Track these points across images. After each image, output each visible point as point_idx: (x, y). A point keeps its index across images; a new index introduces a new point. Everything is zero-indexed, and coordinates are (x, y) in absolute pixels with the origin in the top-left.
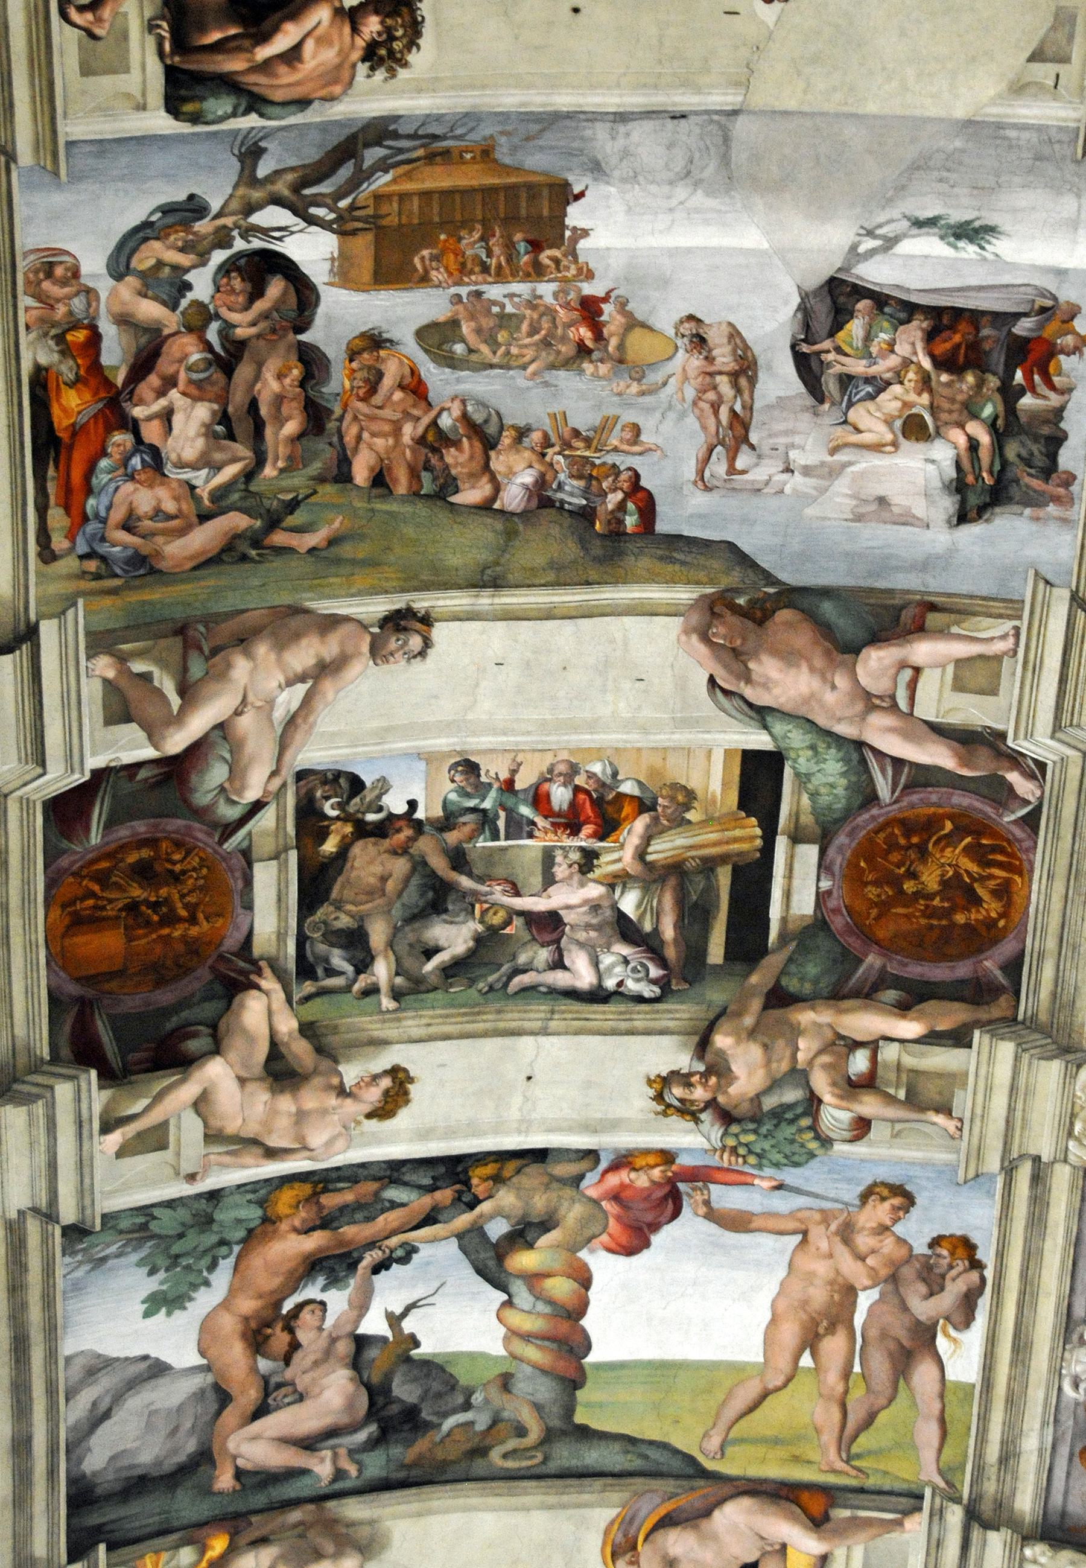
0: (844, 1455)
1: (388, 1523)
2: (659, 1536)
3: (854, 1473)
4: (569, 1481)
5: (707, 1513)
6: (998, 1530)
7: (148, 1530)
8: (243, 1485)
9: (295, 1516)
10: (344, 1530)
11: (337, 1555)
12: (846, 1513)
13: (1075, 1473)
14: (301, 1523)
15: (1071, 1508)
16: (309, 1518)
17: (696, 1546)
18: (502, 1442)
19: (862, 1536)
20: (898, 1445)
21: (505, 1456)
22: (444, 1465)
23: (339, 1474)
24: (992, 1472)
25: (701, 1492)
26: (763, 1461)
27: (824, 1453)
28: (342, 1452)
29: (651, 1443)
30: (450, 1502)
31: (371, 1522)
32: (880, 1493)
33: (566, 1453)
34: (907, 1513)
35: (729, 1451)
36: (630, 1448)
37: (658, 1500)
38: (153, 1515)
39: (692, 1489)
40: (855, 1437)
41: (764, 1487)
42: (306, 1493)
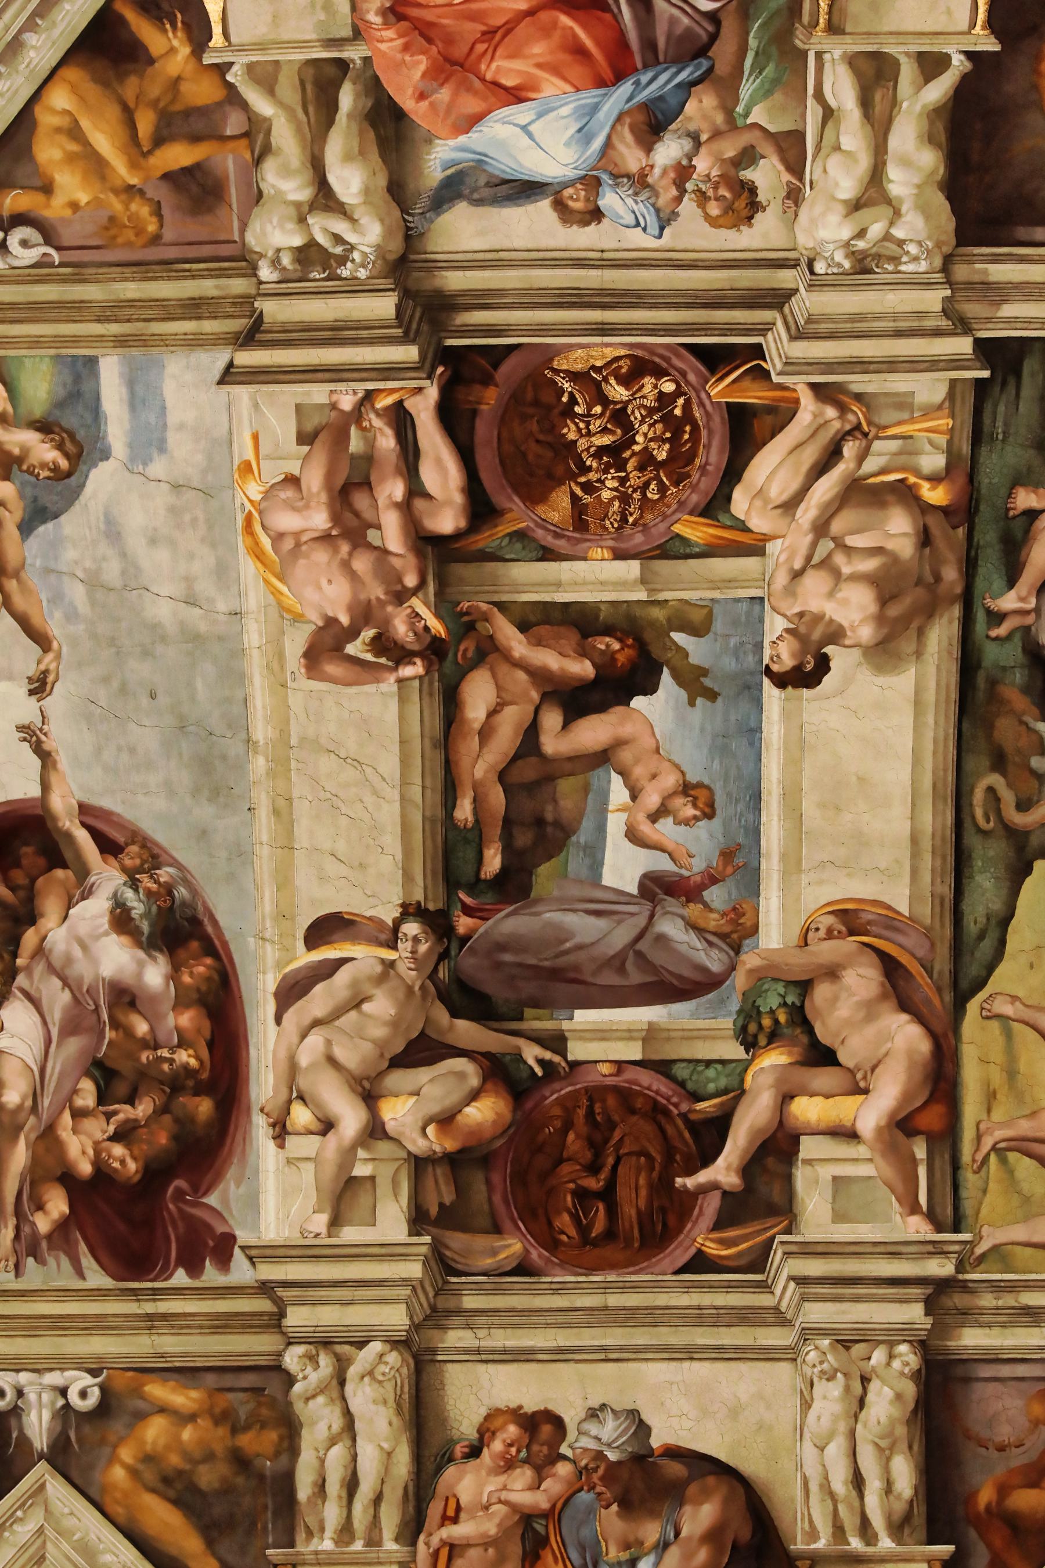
0: (1002, 1145)
1: (913, 670)
2: (875, 959)
3: (979, 1157)
4: (950, 860)
5: (904, 1006)
6: (926, 1314)
7: (987, 421)
8: (1015, 517)
9: (951, 574)
10: (914, 625)
11: (880, 619)
12: (920, 1151)
13: (1023, 1385)
14: (938, 578)
15: (979, 1386)
16: (942, 588)
17: (856, 999)
18: (1010, 785)
19: (889, 1172)
20: (1026, 1200)
21: (991, 790)
22: (989, 727)
23: (997, 618)
24: (1008, 1300)
25: (936, 1001)
26: (984, 1061)
27: (1002, 1125)
28: (1030, 620)
29: (1002, 943)
30: (929, 735)
31: (919, 654)
32: (956, 1187)
33: (991, 853)
34: (931, 1216)
35: (995, 1024)
36: (993, 922)
37: (921, 953)
38: (1006, 424)
39: (939, 990)
40: (1030, 1155)
41: (949, 1067)
42: (980, 584)
